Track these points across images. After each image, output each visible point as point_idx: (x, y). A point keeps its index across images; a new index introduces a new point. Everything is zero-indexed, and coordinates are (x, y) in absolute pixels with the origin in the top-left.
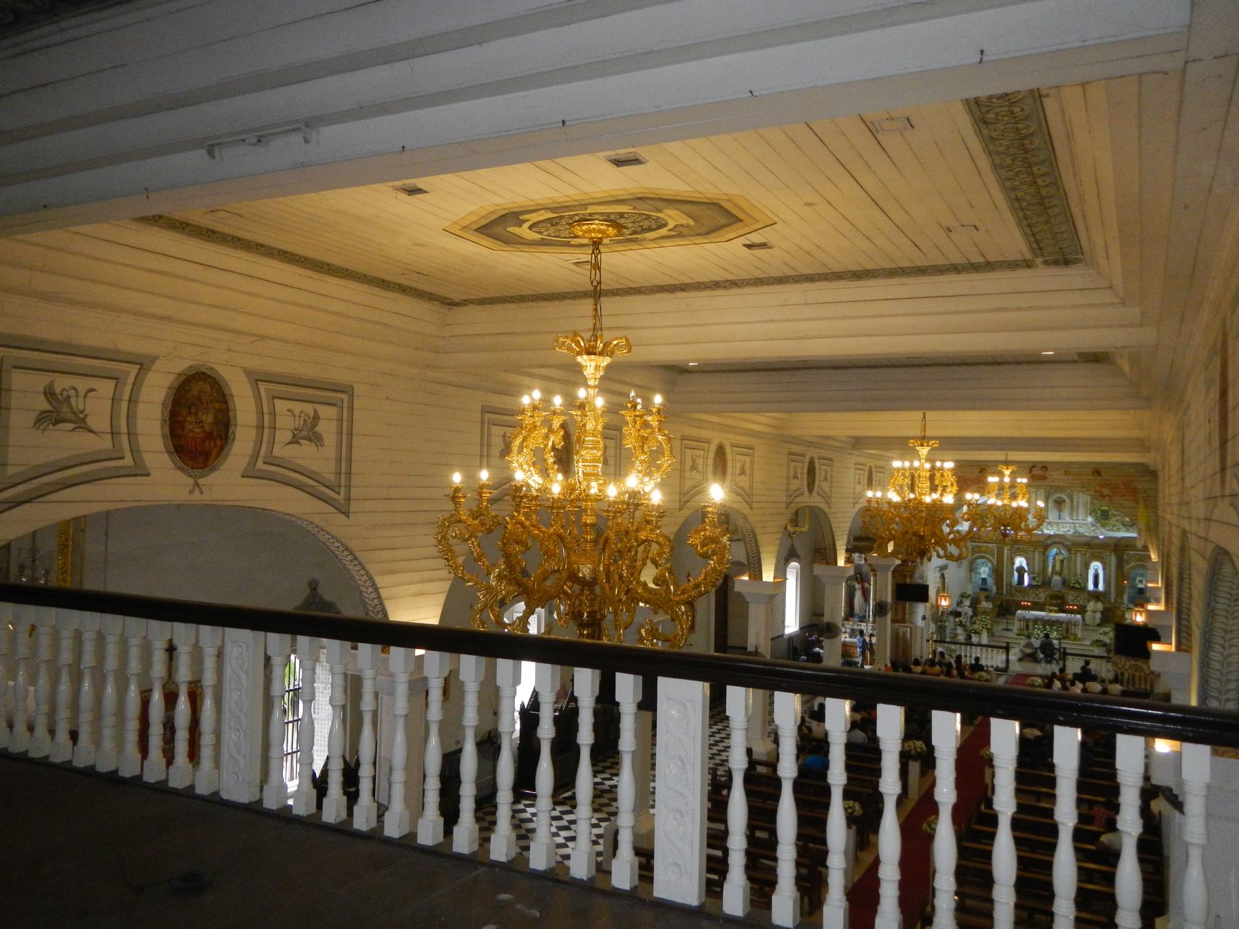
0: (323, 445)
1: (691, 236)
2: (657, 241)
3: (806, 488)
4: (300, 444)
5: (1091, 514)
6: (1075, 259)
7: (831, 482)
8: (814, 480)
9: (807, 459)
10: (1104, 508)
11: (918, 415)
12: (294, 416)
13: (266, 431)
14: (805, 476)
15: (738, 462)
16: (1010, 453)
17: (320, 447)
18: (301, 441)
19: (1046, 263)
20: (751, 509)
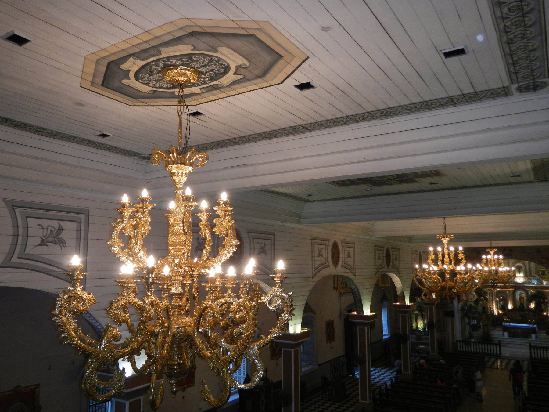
0: (66, 246)
1: (254, 79)
2: (234, 87)
3: (385, 264)
4: (47, 245)
5: (536, 273)
6: (542, 83)
7: (399, 260)
8: (390, 260)
9: (385, 249)
10: (542, 270)
11: (442, 220)
12: (43, 229)
13: (20, 238)
14: (385, 258)
15: (346, 251)
16: (493, 242)
17: (63, 247)
18: (47, 244)
19: (520, 90)
20: (355, 276)
